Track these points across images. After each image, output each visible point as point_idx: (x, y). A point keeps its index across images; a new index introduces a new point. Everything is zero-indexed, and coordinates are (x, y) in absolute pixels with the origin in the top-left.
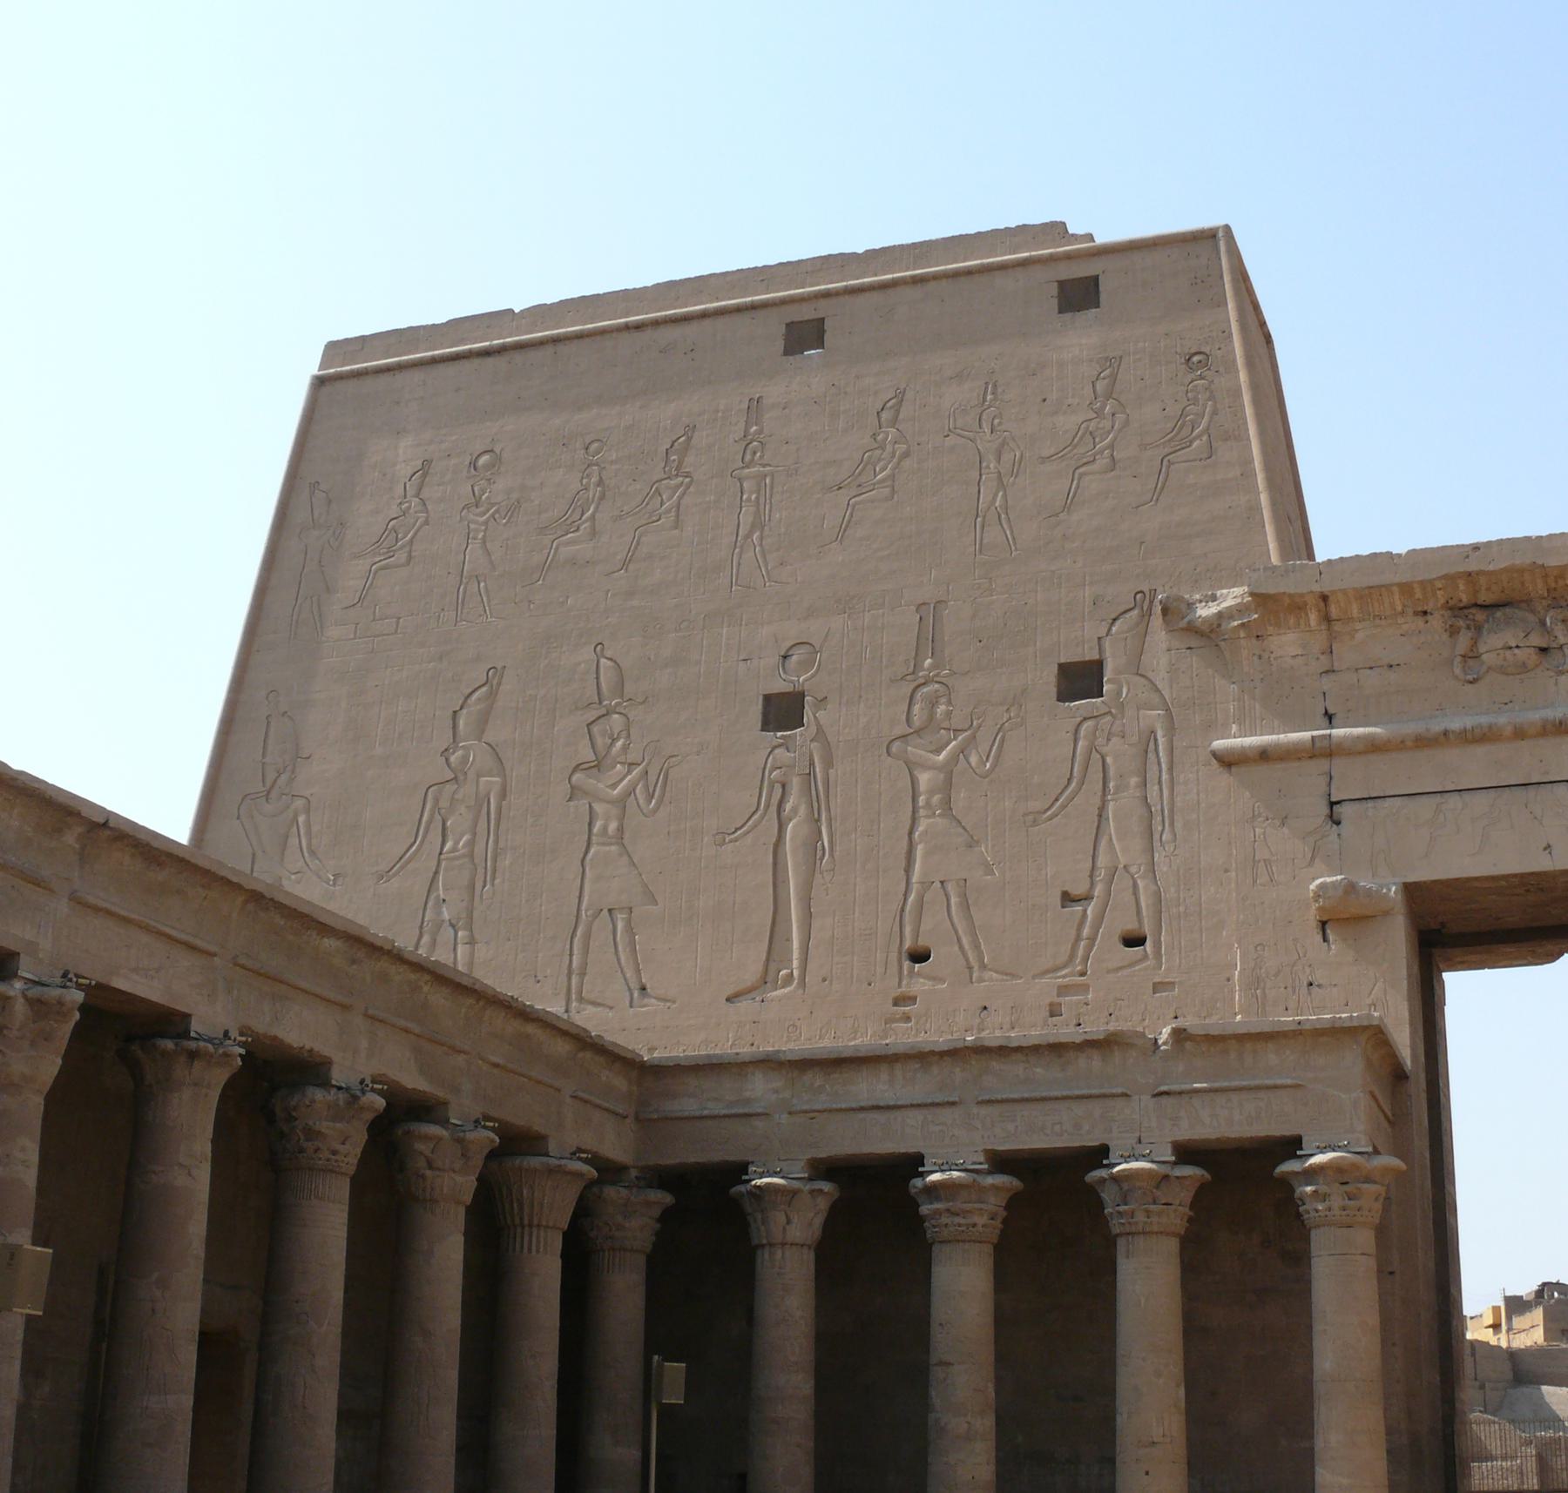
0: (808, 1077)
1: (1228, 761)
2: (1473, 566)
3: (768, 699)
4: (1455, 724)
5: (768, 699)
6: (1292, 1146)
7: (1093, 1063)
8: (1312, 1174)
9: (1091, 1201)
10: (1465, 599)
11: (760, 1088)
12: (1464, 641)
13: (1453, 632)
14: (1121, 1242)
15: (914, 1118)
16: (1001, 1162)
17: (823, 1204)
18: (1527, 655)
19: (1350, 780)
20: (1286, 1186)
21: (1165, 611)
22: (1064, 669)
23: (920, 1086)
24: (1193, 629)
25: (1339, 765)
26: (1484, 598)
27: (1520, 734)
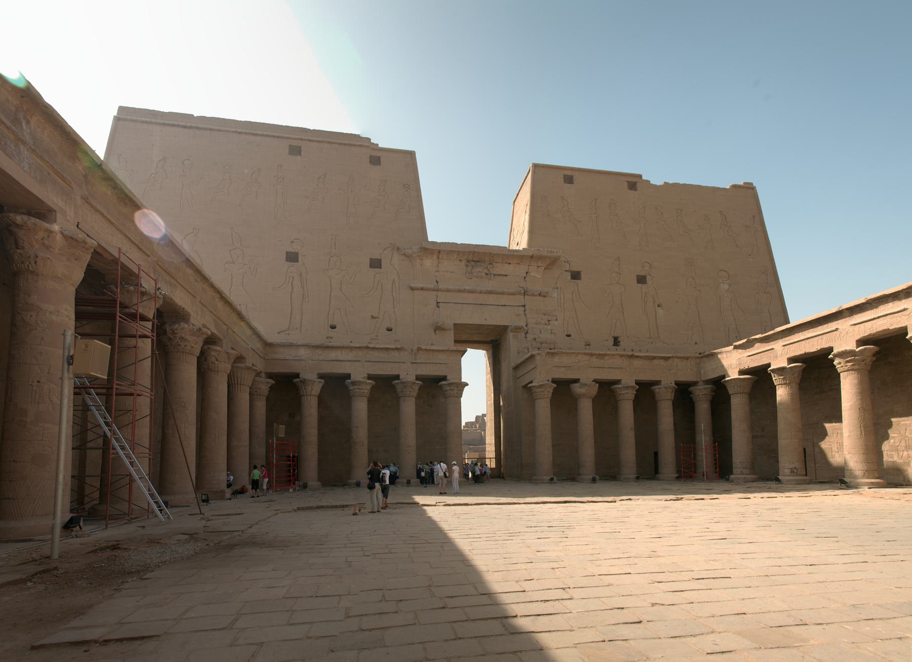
0: (317, 351)
1: (412, 289)
2: (476, 250)
3: (287, 253)
4: (467, 288)
5: (287, 253)
6: (444, 378)
7: (396, 354)
8: (449, 385)
9: (393, 387)
10: (471, 258)
11: (303, 352)
12: (470, 268)
13: (467, 266)
14: (402, 399)
15: (349, 363)
16: (370, 377)
17: (321, 385)
18: (483, 274)
19: (442, 297)
20: (441, 386)
21: (398, 249)
22: (371, 260)
23: (351, 355)
24: (404, 254)
25: (439, 293)
26: (475, 259)
27: (481, 292)
